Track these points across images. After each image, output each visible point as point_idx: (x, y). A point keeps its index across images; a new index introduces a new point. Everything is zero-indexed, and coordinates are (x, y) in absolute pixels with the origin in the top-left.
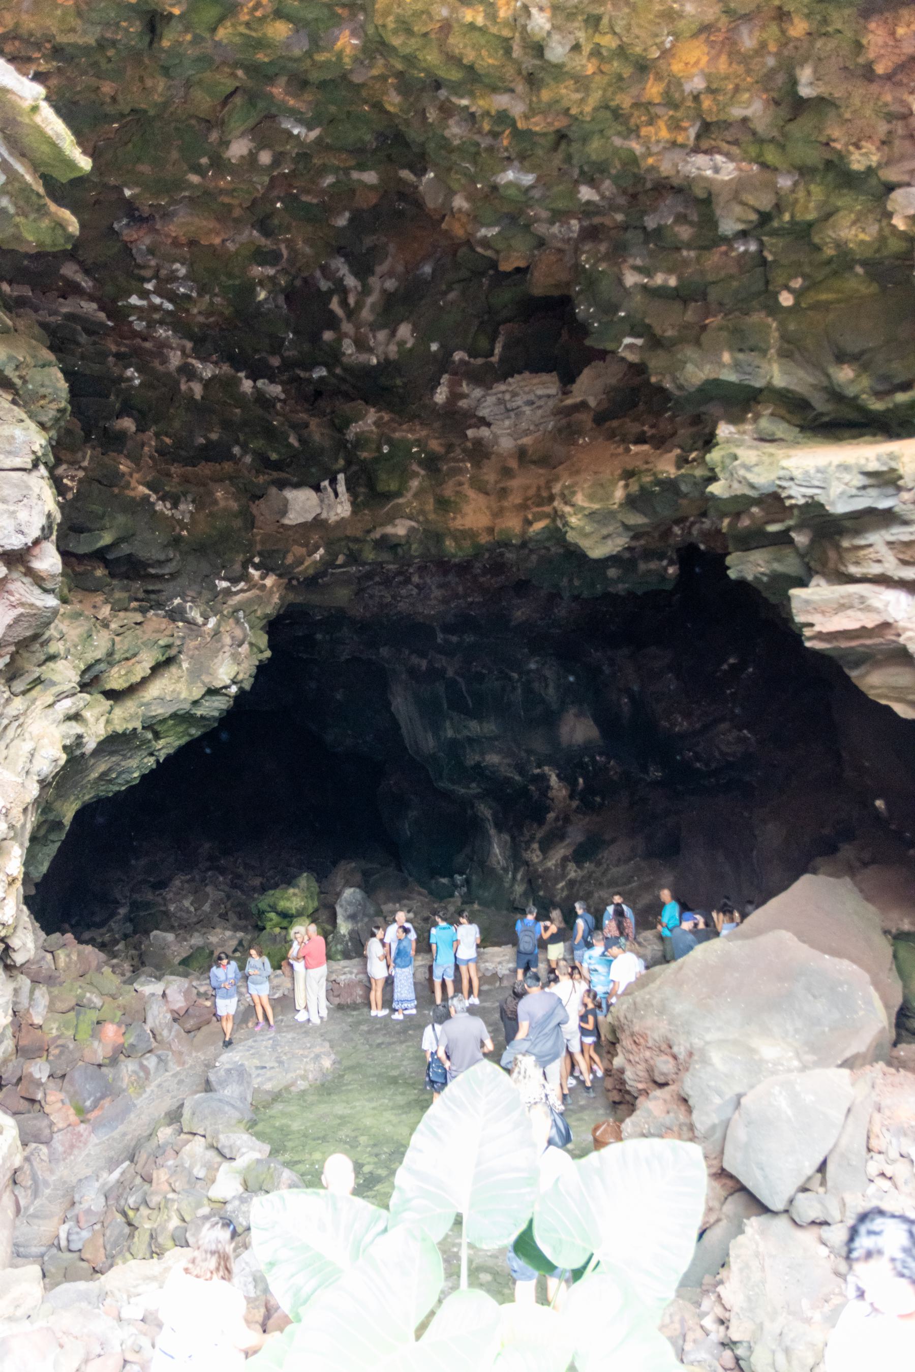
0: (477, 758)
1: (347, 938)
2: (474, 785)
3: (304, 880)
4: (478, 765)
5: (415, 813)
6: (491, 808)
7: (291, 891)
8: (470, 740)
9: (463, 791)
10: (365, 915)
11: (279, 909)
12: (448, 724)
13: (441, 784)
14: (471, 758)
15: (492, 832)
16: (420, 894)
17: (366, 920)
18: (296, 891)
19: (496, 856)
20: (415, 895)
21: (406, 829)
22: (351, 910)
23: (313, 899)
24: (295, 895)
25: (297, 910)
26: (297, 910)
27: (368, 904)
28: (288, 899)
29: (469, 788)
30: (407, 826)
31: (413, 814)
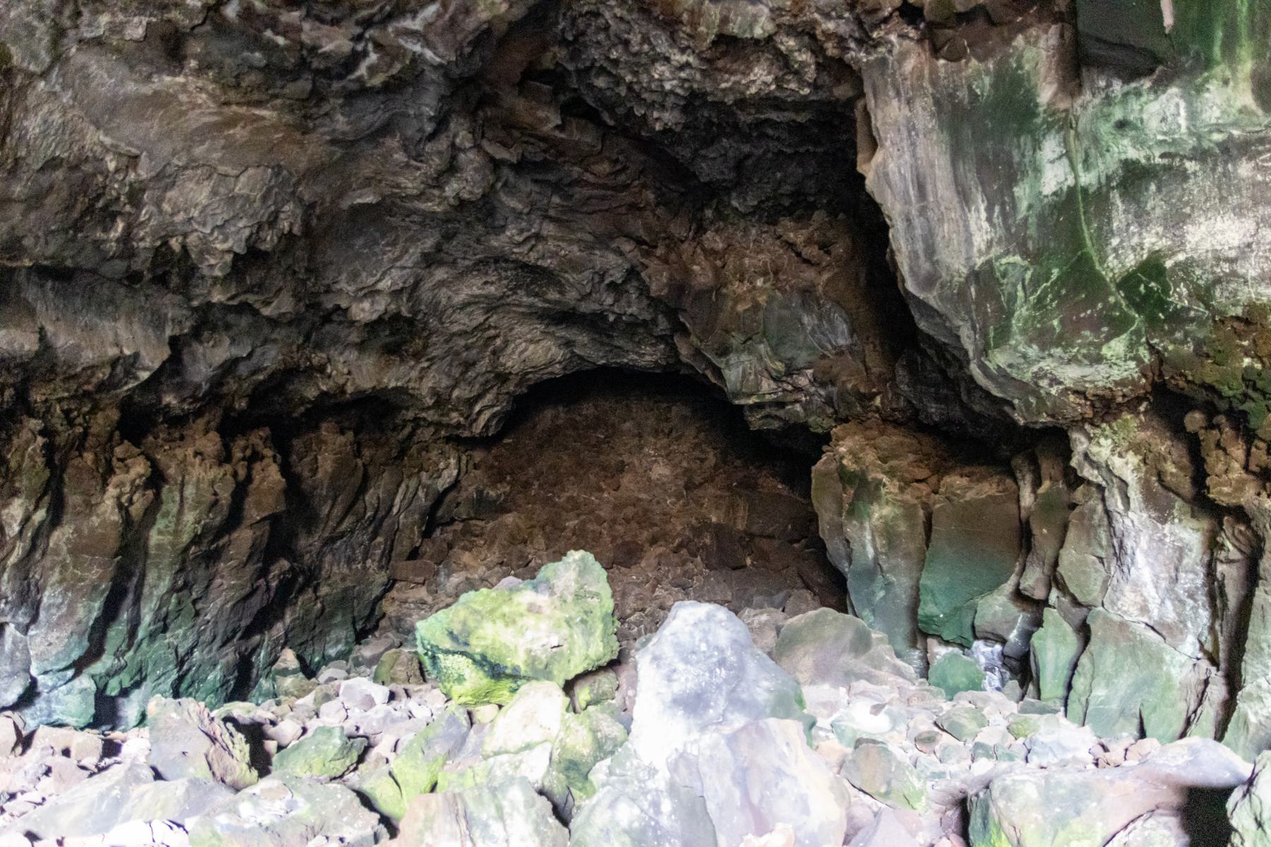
0: (1153, 239)
1: (660, 782)
2: (1118, 346)
3: (576, 572)
4: (1152, 267)
5: (887, 511)
6: (1136, 448)
7: (526, 596)
8: (1134, 177)
9: (1070, 374)
10: (735, 702)
11: (477, 647)
12: (1051, 147)
13: (999, 359)
14: (1127, 244)
15: (1135, 520)
16: (898, 672)
17: (738, 721)
18: (542, 599)
19: (1137, 587)
20: (883, 673)
21: (867, 543)
22: (688, 679)
23: (588, 633)
24: (533, 609)
25: (532, 660)
26: (532, 660)
27: (752, 666)
28: (510, 621)
29: (1099, 359)
30: (868, 537)
31: (880, 512)
